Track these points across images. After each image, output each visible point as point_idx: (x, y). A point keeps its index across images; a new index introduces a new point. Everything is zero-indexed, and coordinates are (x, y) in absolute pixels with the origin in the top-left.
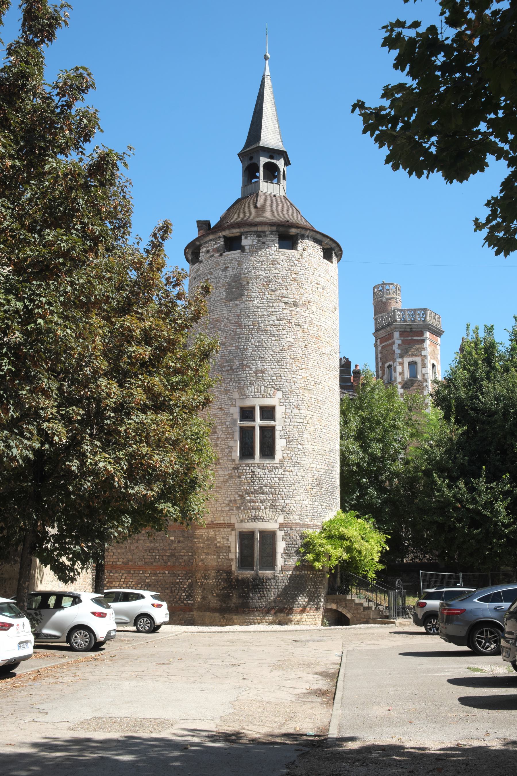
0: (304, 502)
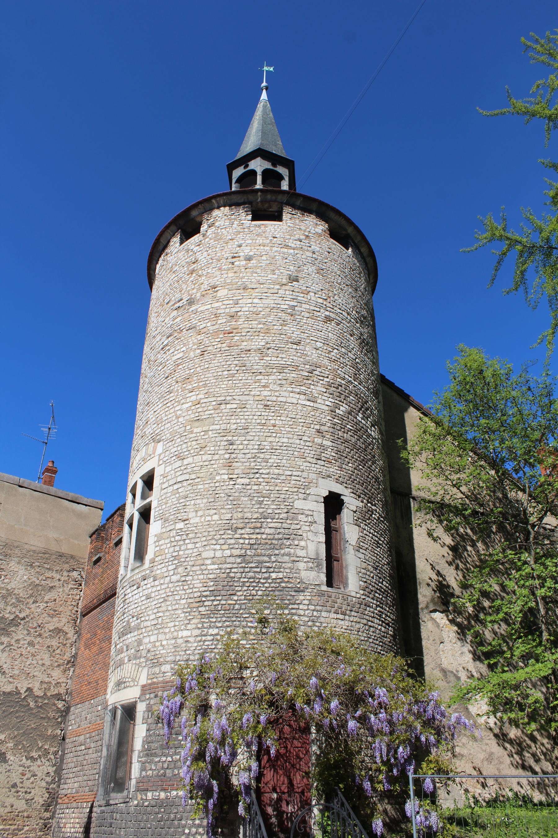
0: (181, 634)
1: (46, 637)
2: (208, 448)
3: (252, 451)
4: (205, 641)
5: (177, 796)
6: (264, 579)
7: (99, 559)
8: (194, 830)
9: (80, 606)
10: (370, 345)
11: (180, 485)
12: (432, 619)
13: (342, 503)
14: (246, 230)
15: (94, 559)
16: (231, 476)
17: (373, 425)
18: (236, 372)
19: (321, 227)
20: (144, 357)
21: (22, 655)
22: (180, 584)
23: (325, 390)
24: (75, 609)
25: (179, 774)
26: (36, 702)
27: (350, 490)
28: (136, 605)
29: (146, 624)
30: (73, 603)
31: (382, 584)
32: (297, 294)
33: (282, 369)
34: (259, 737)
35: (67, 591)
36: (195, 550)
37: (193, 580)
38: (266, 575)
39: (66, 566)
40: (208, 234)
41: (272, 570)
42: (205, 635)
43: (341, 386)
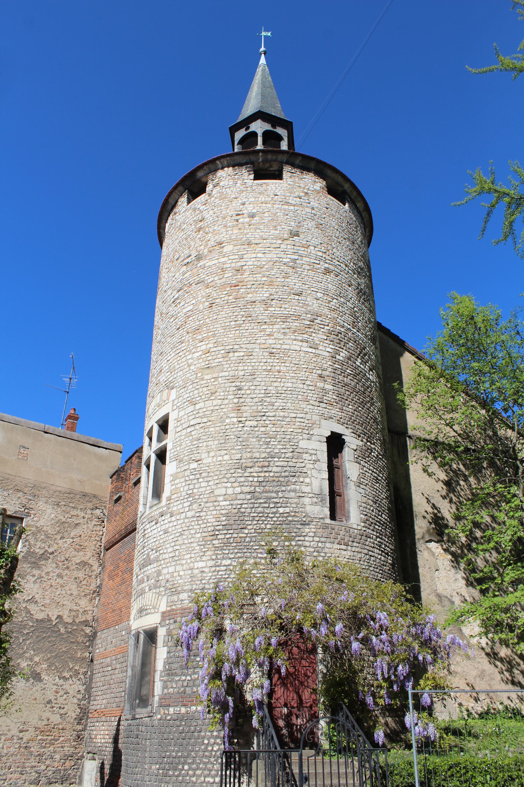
0: (196, 565)
1: (73, 570)
2: (218, 394)
3: (259, 396)
4: (219, 571)
5: (196, 711)
6: (272, 513)
7: (119, 498)
8: (212, 741)
9: (103, 542)
10: (367, 294)
11: (193, 428)
12: (428, 548)
13: (343, 442)
14: (249, 189)
15: (115, 497)
16: (240, 419)
17: (371, 370)
18: (242, 322)
19: (319, 185)
20: (156, 310)
21: (51, 586)
22: (195, 519)
23: (325, 338)
24: (99, 544)
25: (197, 691)
26: (66, 628)
27: (350, 430)
28: (155, 540)
29: (165, 556)
30: (97, 539)
31: (381, 516)
32: (298, 248)
33: (285, 319)
34: (271, 657)
35: (91, 528)
36: (208, 488)
37: (207, 515)
38: (274, 510)
39: (90, 505)
40: (213, 193)
41: (279, 505)
42: (219, 566)
43: (341, 333)
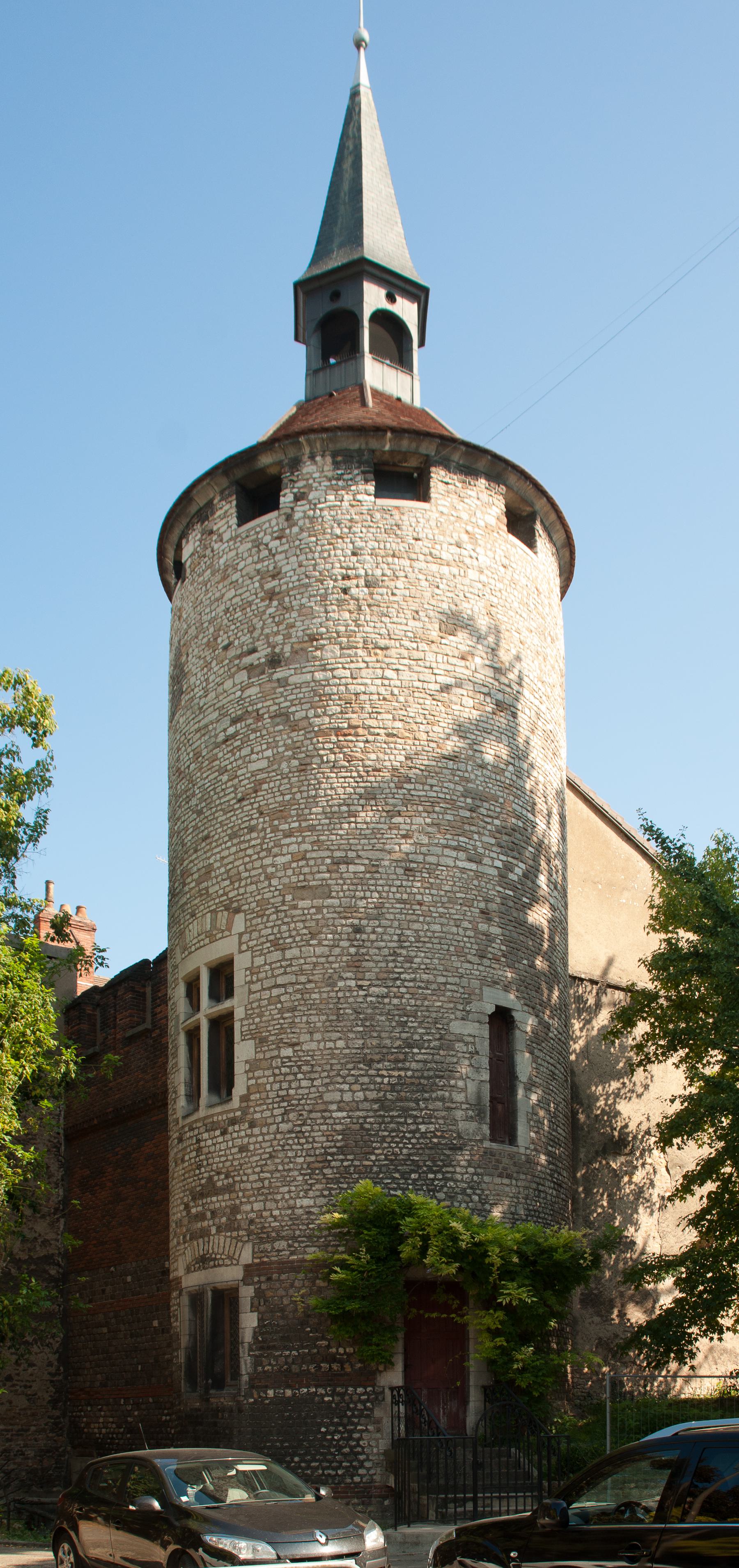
5: (308, 1393)
6: (410, 1132)
16: (360, 983)
36: (313, 1090)
37: (312, 1130)
